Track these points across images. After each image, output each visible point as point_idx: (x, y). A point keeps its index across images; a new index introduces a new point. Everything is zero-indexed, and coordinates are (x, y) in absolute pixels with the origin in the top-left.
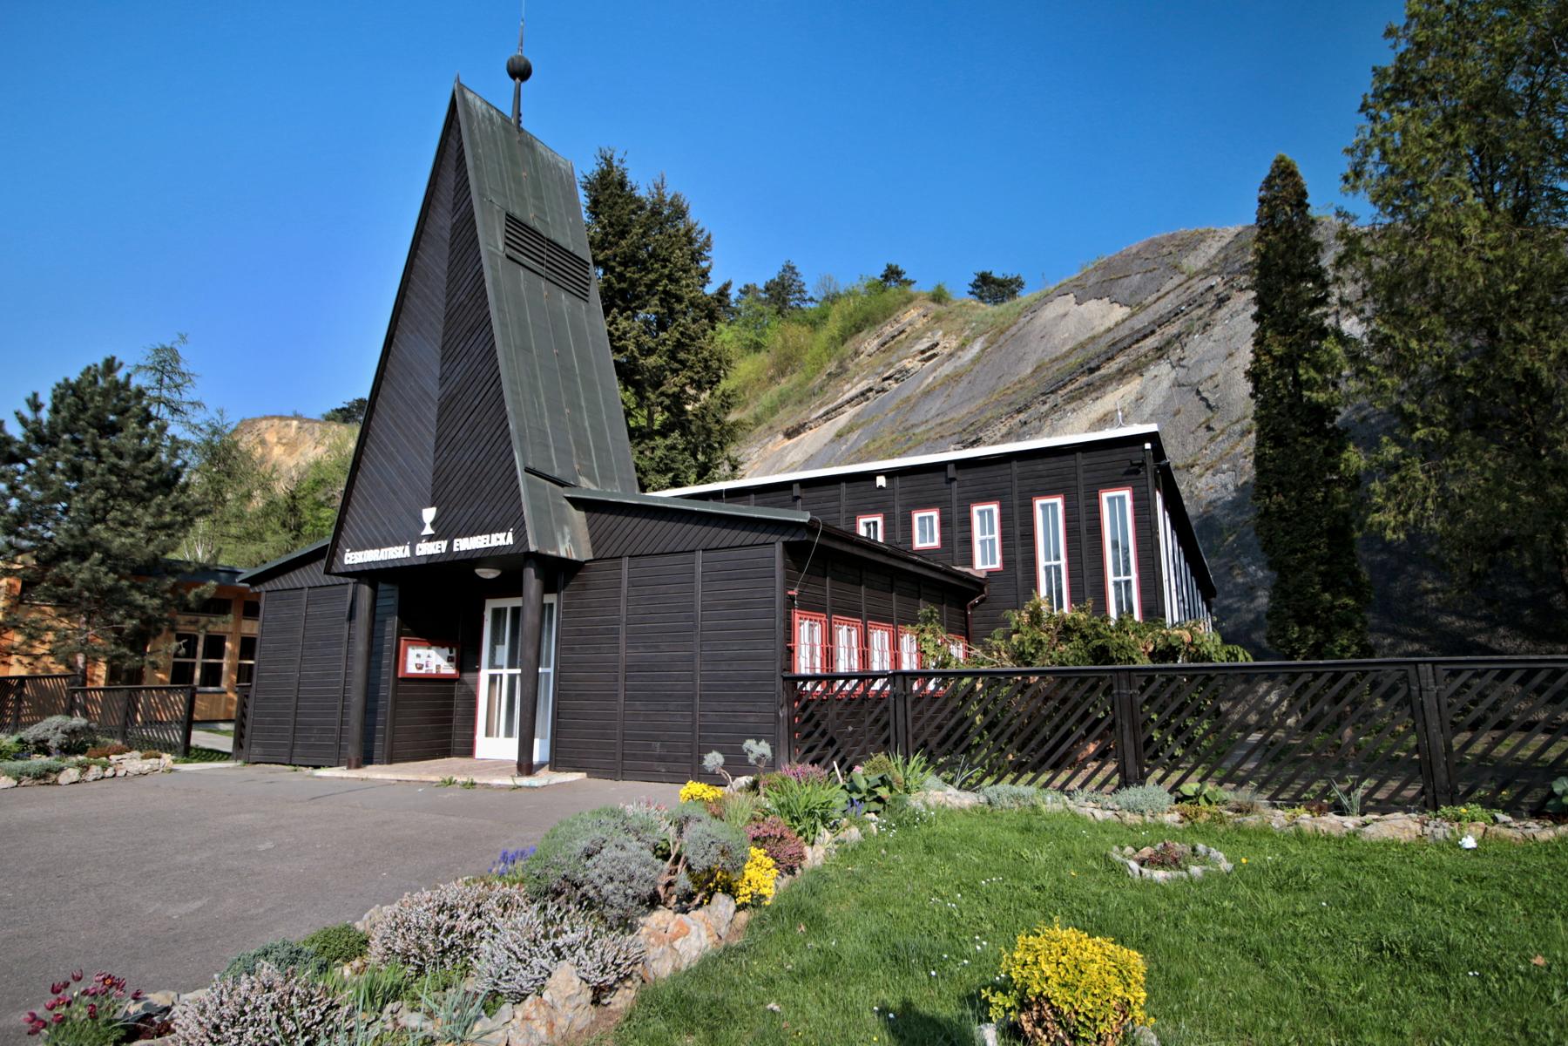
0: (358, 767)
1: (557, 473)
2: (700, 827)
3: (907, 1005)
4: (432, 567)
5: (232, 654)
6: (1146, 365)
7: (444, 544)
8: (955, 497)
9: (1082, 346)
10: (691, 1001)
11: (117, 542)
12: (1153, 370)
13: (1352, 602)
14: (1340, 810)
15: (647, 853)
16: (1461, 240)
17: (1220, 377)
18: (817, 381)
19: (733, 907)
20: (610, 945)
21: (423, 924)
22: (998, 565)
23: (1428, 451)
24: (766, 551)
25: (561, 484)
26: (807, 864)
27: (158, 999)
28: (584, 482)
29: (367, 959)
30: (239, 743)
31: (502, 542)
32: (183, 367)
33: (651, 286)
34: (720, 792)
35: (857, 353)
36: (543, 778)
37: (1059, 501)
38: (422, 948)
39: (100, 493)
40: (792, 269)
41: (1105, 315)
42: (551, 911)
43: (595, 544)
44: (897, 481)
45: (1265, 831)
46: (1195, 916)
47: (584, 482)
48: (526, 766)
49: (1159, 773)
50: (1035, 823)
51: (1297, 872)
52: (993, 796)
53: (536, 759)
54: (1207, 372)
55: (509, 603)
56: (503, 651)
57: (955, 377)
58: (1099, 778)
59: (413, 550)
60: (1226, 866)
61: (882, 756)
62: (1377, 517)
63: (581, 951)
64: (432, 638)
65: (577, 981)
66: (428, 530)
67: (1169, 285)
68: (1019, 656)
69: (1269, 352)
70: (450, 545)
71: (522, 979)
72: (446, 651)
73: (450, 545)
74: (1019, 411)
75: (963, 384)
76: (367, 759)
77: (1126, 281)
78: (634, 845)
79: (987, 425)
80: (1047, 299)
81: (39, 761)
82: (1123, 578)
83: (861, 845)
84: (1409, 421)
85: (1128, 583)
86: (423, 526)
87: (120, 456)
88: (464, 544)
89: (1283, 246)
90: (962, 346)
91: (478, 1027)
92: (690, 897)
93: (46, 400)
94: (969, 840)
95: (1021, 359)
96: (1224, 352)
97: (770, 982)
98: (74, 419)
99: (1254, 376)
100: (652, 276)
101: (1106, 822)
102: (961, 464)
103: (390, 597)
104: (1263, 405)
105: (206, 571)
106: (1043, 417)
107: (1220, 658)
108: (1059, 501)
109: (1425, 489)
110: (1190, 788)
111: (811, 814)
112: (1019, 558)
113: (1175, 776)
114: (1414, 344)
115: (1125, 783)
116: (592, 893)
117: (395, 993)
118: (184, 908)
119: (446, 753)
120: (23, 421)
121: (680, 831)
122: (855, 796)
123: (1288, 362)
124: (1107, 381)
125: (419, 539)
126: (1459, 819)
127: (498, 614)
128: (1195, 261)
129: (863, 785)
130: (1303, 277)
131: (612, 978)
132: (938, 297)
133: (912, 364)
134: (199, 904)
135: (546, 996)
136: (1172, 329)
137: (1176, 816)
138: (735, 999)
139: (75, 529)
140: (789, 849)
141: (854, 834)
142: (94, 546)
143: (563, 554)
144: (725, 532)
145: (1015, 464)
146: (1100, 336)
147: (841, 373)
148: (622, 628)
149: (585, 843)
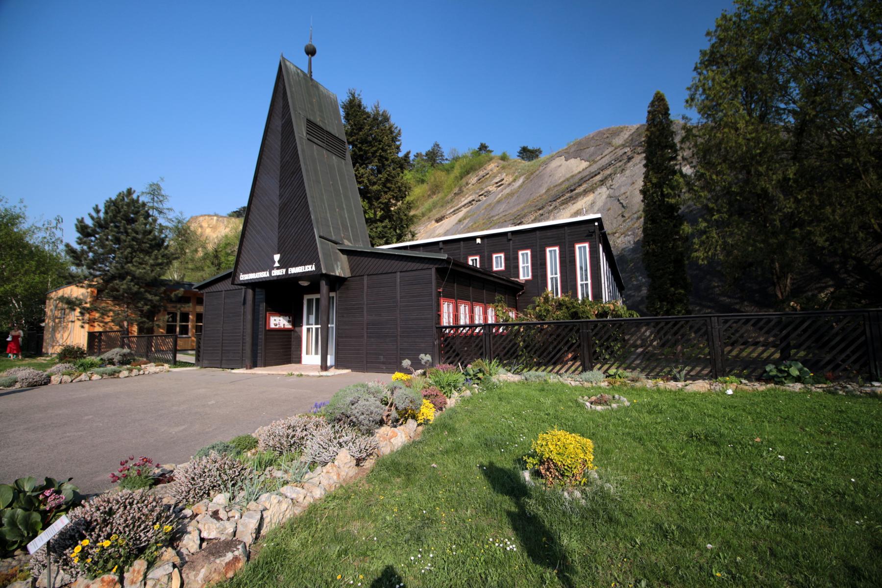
0: (251, 368)
1: (334, 238)
2: (401, 391)
3: (491, 464)
4: (279, 280)
5: (193, 321)
6: (596, 188)
7: (284, 270)
8: (511, 247)
9: (568, 180)
10: (400, 464)
11: (138, 271)
12: (599, 190)
13: (683, 292)
14: (676, 379)
15: (378, 403)
16: (737, 129)
17: (628, 193)
18: (450, 197)
19: (416, 424)
20: (363, 441)
21: (281, 434)
22: (530, 277)
23: (719, 224)
24: (428, 272)
25: (336, 243)
26: (448, 406)
27: (167, 467)
28: (346, 242)
29: (258, 449)
30: (198, 360)
31: (310, 269)
32: (163, 193)
33: (374, 153)
34: (409, 377)
35: (467, 184)
36: (332, 372)
37: (557, 249)
38: (281, 444)
39: (129, 250)
40: (438, 145)
41: (578, 166)
42: (337, 427)
43: (352, 270)
44: (486, 240)
45: (644, 389)
46: (614, 424)
47: (346, 242)
48: (324, 367)
49: (599, 366)
50: (546, 388)
51: (657, 406)
52: (528, 376)
53: (329, 364)
54: (622, 191)
55: (314, 297)
56: (313, 318)
57: (511, 194)
58: (573, 368)
59: (270, 273)
60: (627, 404)
61: (480, 360)
62: (695, 254)
63: (351, 444)
64: (281, 313)
65: (349, 456)
66: (277, 265)
67: (606, 152)
68: (539, 317)
69: (650, 181)
70: (287, 271)
71: (325, 456)
72: (287, 318)
73: (287, 271)
74: (539, 209)
75: (515, 197)
76: (254, 365)
77: (588, 150)
78: (372, 399)
79: (525, 216)
80: (552, 158)
81: (110, 368)
82: (584, 282)
83: (471, 398)
84: (710, 211)
85: (587, 285)
86: (274, 262)
87: (137, 233)
88: (293, 270)
89: (658, 133)
90: (514, 180)
91: (307, 476)
92: (397, 421)
93: (102, 208)
94: (517, 395)
95: (541, 186)
96: (630, 182)
97: (433, 455)
98: (115, 216)
99: (644, 192)
100: (374, 149)
101: (576, 386)
102: (513, 233)
103: (261, 294)
104: (647, 205)
105: (178, 284)
106: (550, 212)
107: (626, 316)
108: (557, 249)
109: (717, 241)
110: (612, 371)
111: (449, 385)
112: (539, 274)
113: (606, 367)
114: (714, 177)
115: (585, 370)
116: (354, 420)
117: (270, 463)
118: (177, 429)
119: (289, 362)
120: (92, 218)
121: (392, 393)
122: (468, 377)
123: (659, 186)
124: (579, 195)
125: (273, 268)
126: (726, 382)
127: (310, 301)
128: (618, 141)
129: (471, 372)
130: (666, 147)
131: (364, 455)
132: (504, 158)
133: (492, 188)
134: (183, 427)
135: (336, 463)
136: (608, 172)
137: (606, 383)
138: (418, 463)
139: (119, 266)
140: (440, 400)
141: (468, 393)
142: (128, 273)
143: (337, 274)
144: (409, 264)
145: (538, 232)
146: (576, 175)
147: (460, 193)
148: (365, 307)
149: (351, 399)
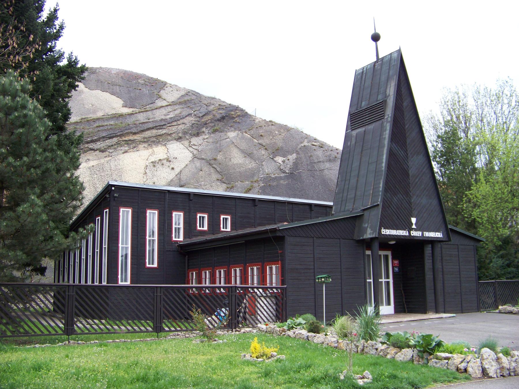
7: (421, 233)
31: (439, 236)
59: (409, 233)
70: (423, 234)
73: (423, 234)
85: (153, 241)
86: (412, 224)
